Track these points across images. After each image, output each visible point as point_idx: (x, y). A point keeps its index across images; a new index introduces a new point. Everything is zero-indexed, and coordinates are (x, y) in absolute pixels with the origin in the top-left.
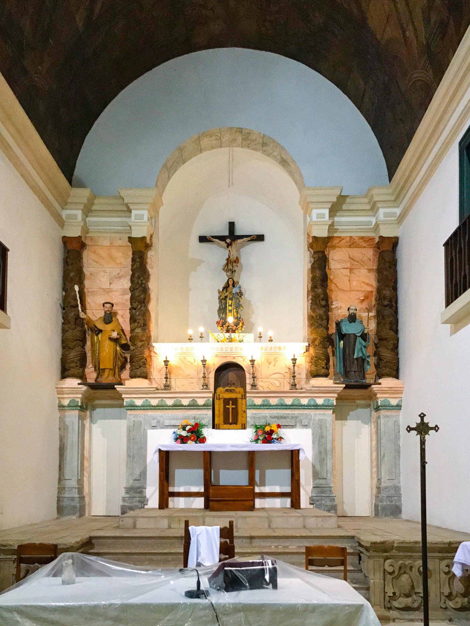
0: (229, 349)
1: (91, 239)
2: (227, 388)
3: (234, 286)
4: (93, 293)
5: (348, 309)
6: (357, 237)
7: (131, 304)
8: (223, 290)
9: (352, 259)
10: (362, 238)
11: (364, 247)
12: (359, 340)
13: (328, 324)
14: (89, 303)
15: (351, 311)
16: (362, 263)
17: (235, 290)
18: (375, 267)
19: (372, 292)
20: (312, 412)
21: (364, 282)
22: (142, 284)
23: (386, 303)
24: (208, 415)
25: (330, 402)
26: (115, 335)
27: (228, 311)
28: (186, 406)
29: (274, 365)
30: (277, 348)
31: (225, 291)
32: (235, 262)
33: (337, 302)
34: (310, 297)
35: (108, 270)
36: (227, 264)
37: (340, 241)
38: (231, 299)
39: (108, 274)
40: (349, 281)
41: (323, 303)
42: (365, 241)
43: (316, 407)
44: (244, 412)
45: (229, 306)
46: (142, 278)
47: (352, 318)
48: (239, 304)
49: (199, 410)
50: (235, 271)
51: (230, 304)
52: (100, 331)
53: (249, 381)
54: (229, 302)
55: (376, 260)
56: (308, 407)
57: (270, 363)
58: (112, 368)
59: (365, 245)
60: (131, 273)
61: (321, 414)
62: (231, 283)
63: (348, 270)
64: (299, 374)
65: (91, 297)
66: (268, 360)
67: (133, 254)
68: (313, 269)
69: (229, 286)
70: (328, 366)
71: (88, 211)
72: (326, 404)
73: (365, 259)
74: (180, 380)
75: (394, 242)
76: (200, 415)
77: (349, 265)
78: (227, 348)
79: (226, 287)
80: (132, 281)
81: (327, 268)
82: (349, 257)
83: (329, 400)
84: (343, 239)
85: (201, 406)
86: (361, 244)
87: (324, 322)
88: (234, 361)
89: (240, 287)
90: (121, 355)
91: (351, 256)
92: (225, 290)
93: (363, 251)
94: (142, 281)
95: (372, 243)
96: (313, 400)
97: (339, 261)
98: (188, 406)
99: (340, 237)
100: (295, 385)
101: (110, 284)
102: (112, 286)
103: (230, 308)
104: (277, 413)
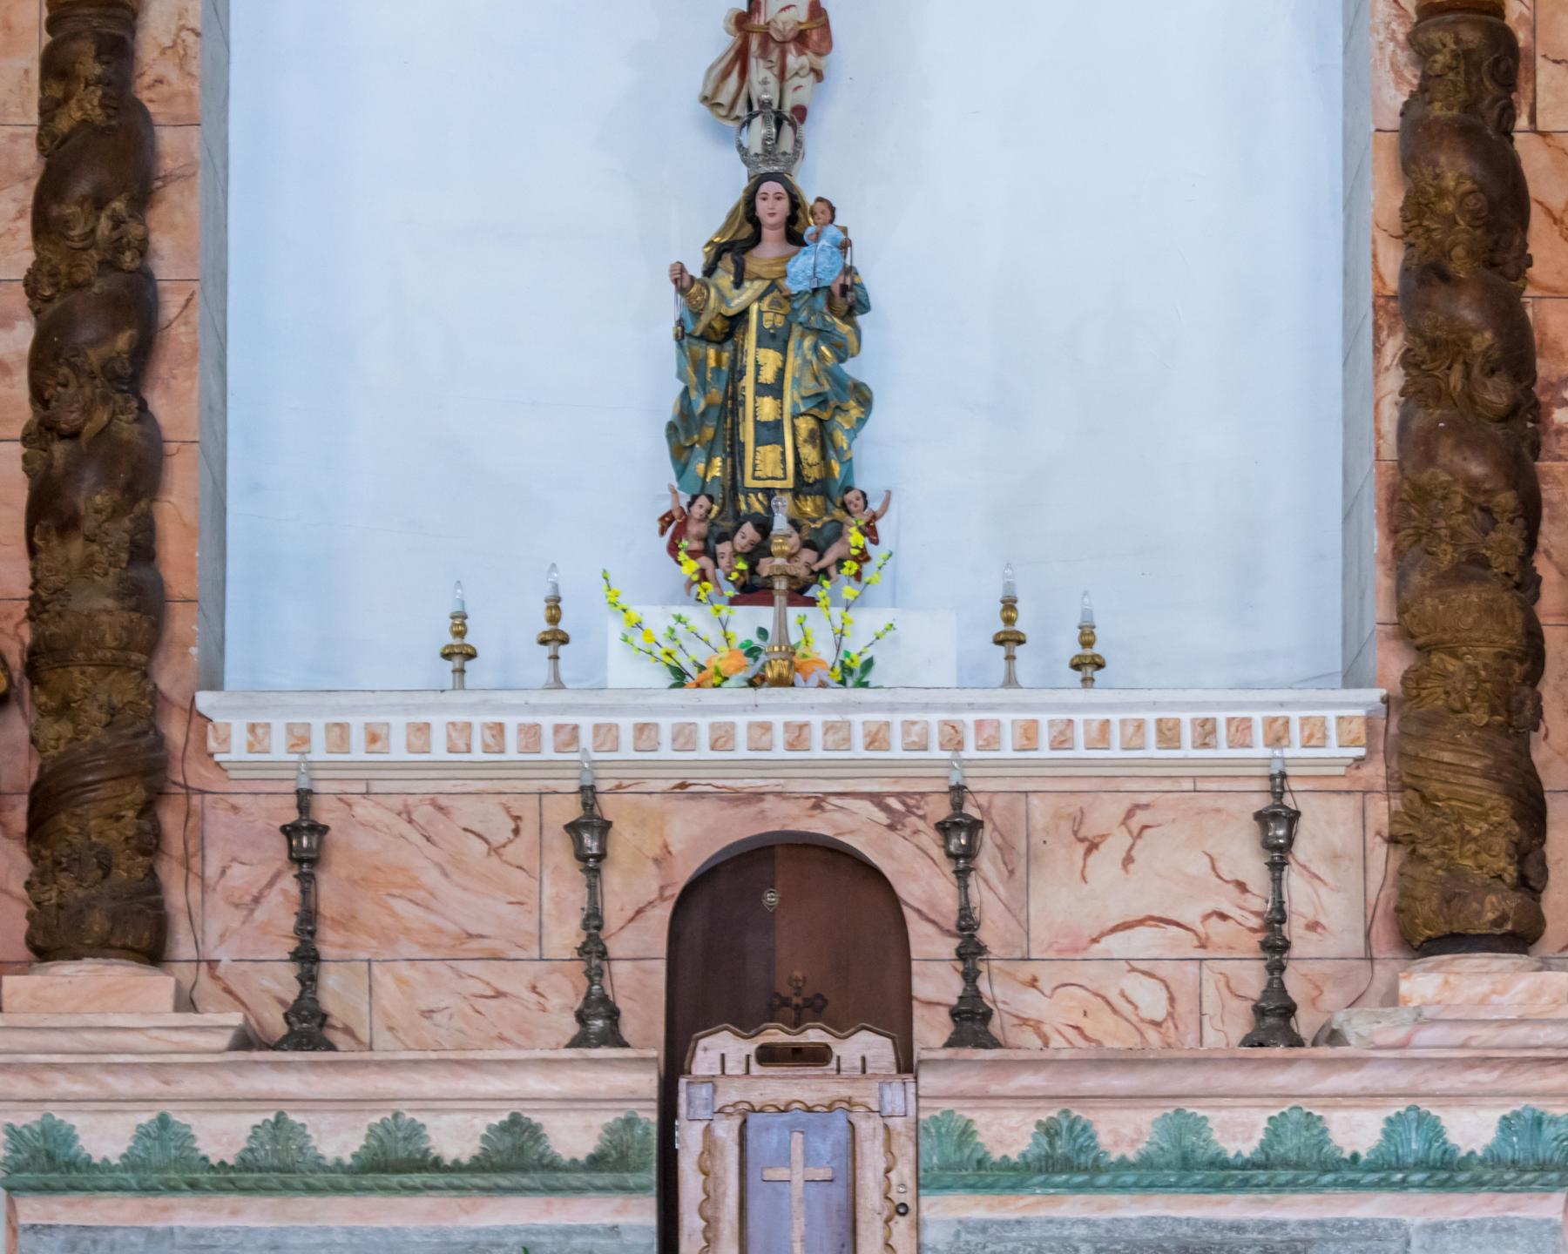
0: (779, 736)
2: (776, 1036)
3: (794, 236)
7: (39, 396)
8: (710, 271)
13: (1531, 542)
17: (803, 269)
20: (1414, 1210)
22: (118, 246)
24: (629, 1239)
25: (1549, 1132)
27: (748, 433)
28: (457, 1167)
29: (1128, 860)
30: (1151, 734)
31: (724, 279)
32: (801, 39)
34: (1394, 346)
36: (741, 56)
38: (775, 339)
41: (1497, 393)
43: (1445, 1171)
44: (902, 1210)
45: (762, 390)
46: (118, 205)
48: (839, 381)
49: (556, 1201)
50: (801, 112)
51: (768, 376)
53: (935, 980)
54: (762, 361)
56: (1380, 1171)
57: (1093, 847)
60: (29, 159)
61: (1480, 1225)
62: (772, 209)
64: (1313, 926)
66: (1078, 820)
67: (52, 25)
68: (1417, 138)
69: (756, 239)
70: (1531, 871)
72: (1517, 1148)
74: (405, 970)
76: (568, 1232)
78: (766, 727)
79: (735, 246)
80: (44, 225)
81: (1522, 122)
83: (1538, 1122)
85: (574, 1166)
87: (1508, 535)
88: (819, 826)
89: (845, 246)
92: (727, 262)
94: (117, 223)
96: (1423, 1119)
98: (478, 1166)
100: (1289, 1010)
103: (768, 408)
104: (1150, 1223)
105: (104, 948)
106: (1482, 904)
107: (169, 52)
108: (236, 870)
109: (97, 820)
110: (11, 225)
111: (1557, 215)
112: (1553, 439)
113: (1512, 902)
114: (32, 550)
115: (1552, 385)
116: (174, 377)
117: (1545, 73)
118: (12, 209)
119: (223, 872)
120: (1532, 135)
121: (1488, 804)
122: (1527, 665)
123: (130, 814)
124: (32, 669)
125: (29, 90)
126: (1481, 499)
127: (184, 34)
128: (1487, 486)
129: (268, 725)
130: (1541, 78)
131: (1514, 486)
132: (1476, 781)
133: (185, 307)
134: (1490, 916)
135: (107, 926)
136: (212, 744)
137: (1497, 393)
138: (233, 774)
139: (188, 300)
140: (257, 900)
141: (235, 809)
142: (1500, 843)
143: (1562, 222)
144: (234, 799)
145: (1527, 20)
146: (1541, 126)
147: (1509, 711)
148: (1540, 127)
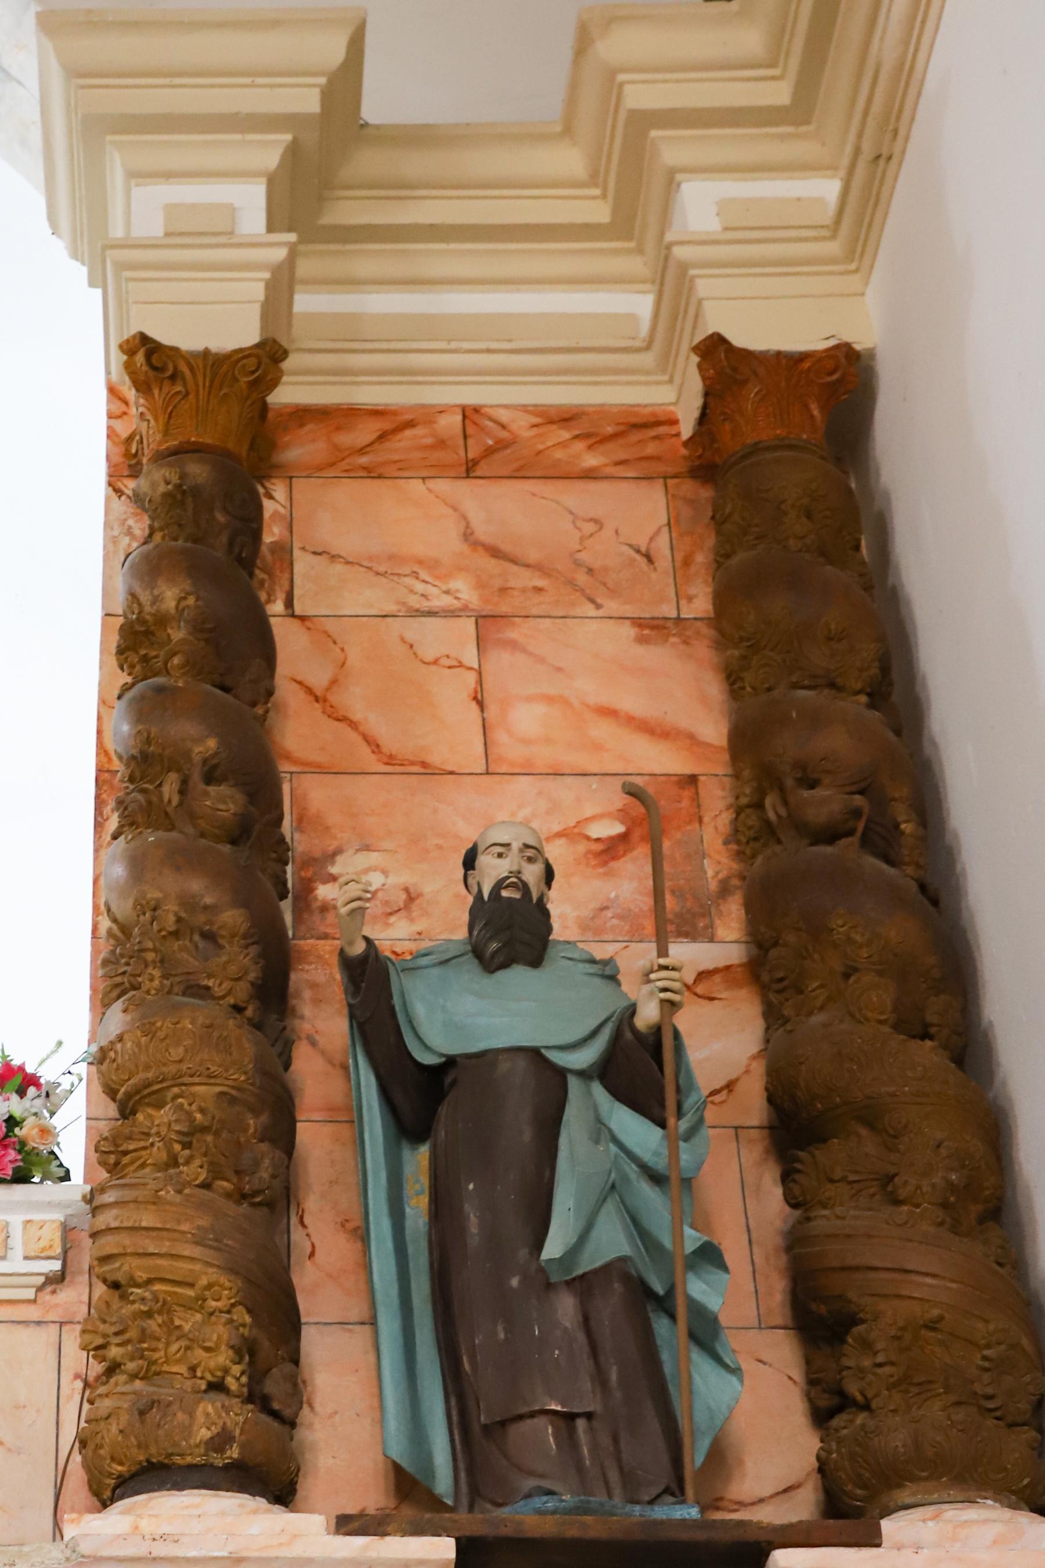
5: (470, 862)
6: (524, 408)
9: (495, 552)
10: (564, 417)
11: (590, 475)
12: (589, 1105)
15: (492, 869)
16: (582, 583)
18: (700, 603)
19: (692, 780)
21: (609, 713)
23: (825, 803)
33: (374, 858)
37: (383, 437)
40: (481, 704)
41: (223, 802)
42: (596, 440)
47: (511, 930)
55: (700, 558)
59: (591, 460)
63: (469, 626)
73: (606, 551)
75: (837, 391)
77: (464, 590)
82: (468, 535)
84: (411, 424)
86: (559, 454)
91: (483, 531)
93: (577, 497)
95: (651, 449)
97: (386, 566)
99: (377, 413)
106: (191, 1415)
111: (318, 694)
112: (316, 918)
113: (238, 1416)
115: (315, 860)
117: (302, 564)
120: (290, 620)
121: (204, 1281)
122: (264, 1118)
126: (201, 918)
128: (208, 900)
130: (298, 568)
131: (244, 904)
132: (187, 1250)
134: (204, 1434)
137: (223, 802)
142: (219, 1332)
143: (325, 701)
145: (282, 517)
146: (298, 611)
147: (237, 1172)
148: (298, 612)
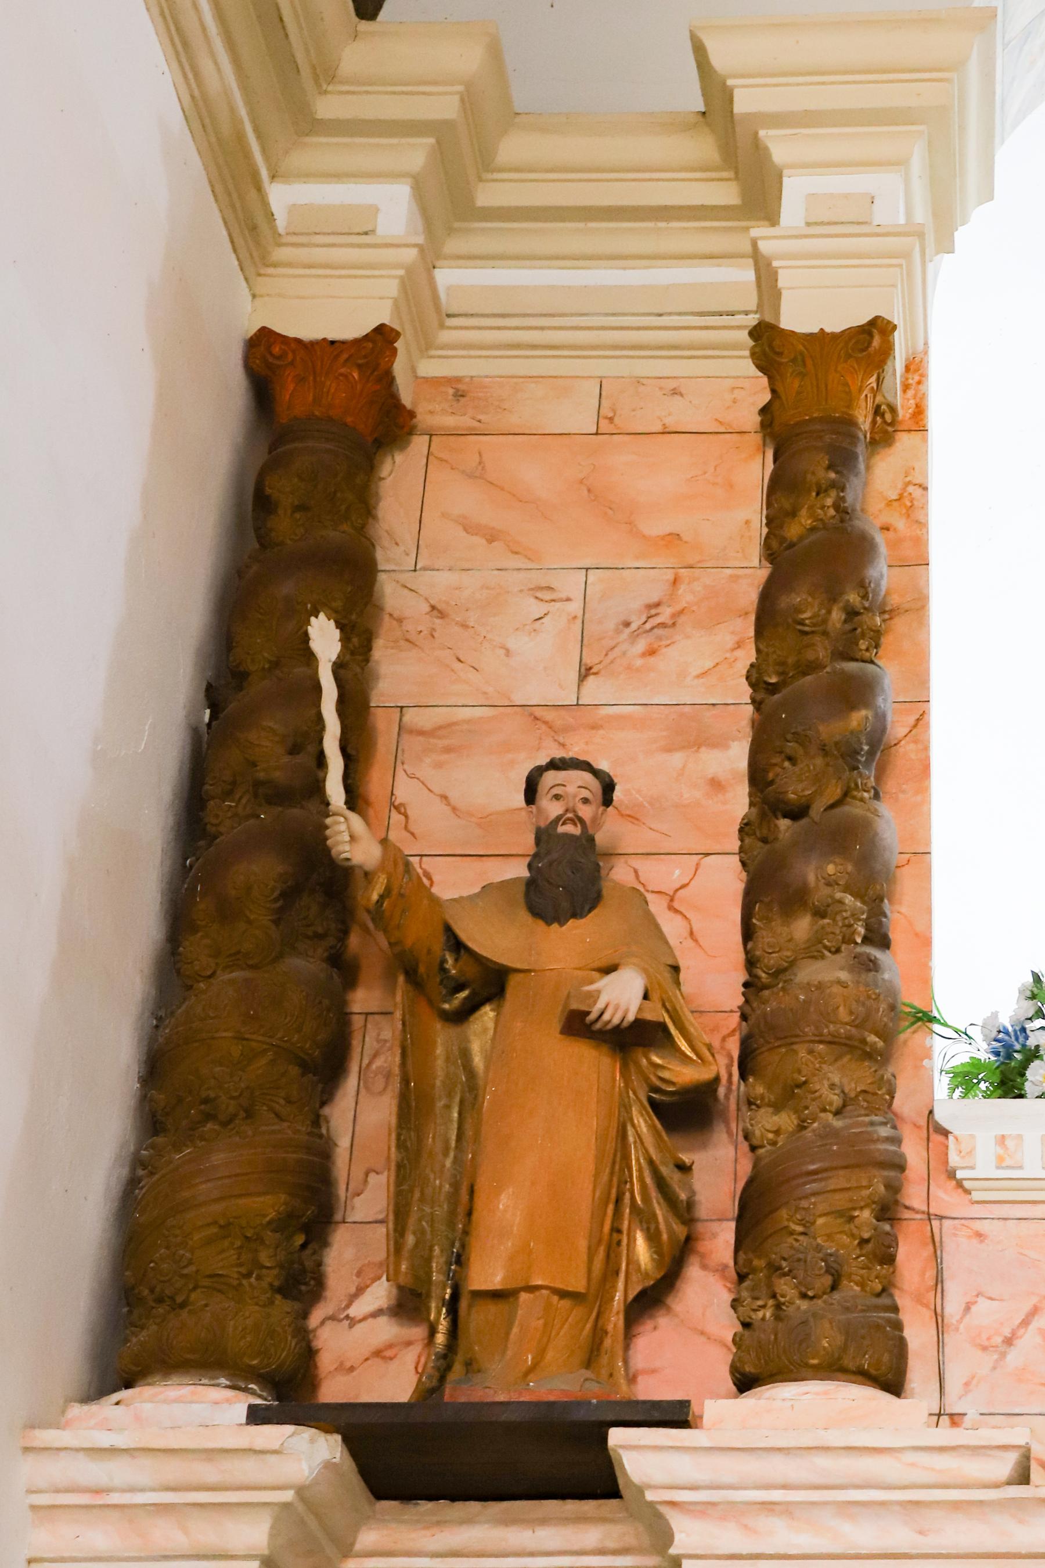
1: (459, 395)
4: (449, 740)
14: (400, 809)
26: (621, 996)
35: (571, 584)
39: (575, 607)
52: (492, 983)
58: (578, 1284)
65: (425, 770)
71: (451, 203)
90: (661, 1184)
101: (585, 673)
102: (595, 691)
105: (834, 1369)
107: (895, 504)
108: (983, 1306)
109: (819, 1224)
110: (728, 655)
114: (748, 933)
116: (903, 792)
118: (730, 640)
119: (968, 1308)
123: (866, 1214)
124: (747, 1064)
125: (750, 538)
127: (911, 489)
129: (1020, 1137)
133: (915, 726)
135: (840, 1340)
136: (954, 1159)
138: (976, 1196)
139: (918, 720)
140: (1009, 1341)
141: (979, 1235)
144: (978, 1226)
